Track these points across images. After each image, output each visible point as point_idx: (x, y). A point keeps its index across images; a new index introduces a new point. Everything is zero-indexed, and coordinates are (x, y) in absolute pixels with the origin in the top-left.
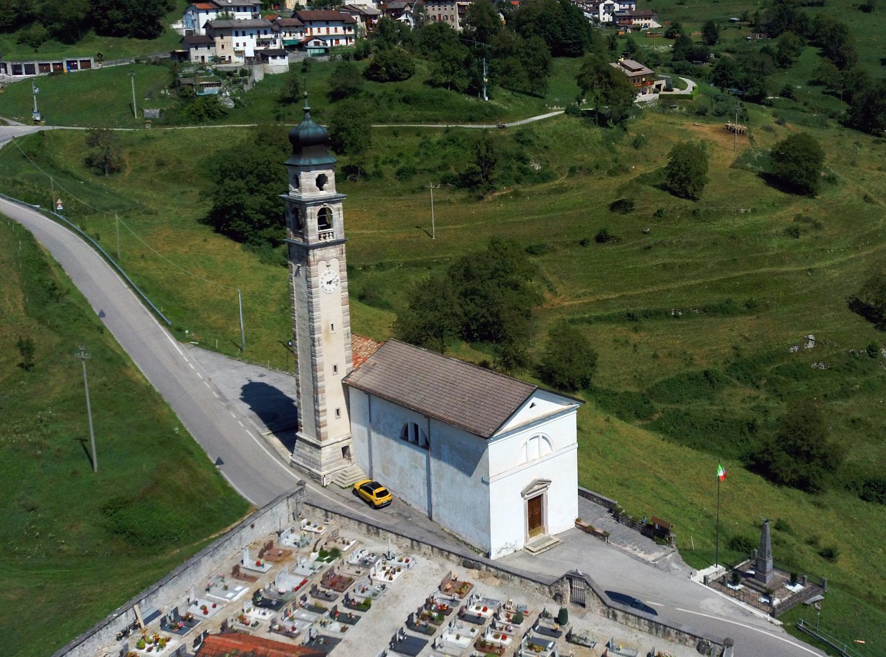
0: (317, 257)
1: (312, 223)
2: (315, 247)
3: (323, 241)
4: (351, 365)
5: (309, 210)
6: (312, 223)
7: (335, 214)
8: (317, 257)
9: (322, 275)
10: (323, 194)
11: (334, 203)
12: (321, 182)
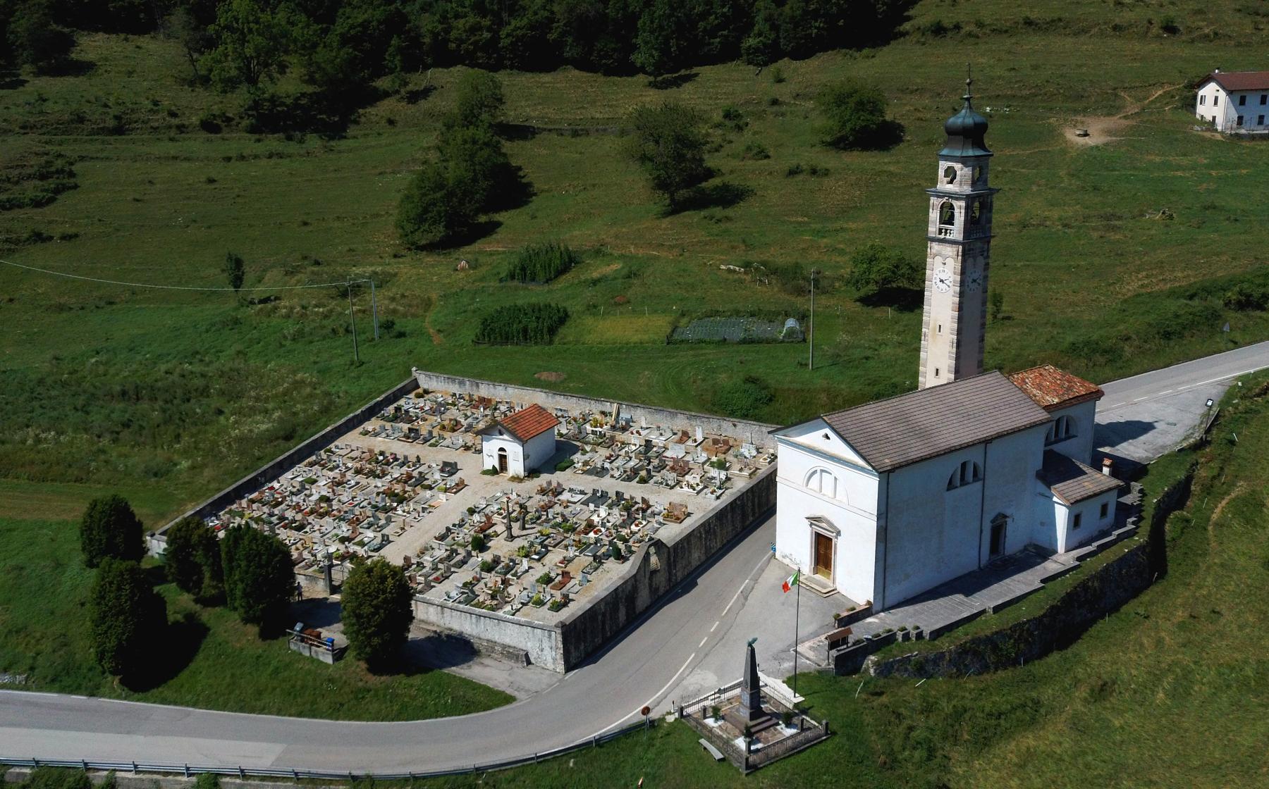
0: (934, 251)
1: (934, 215)
2: (933, 240)
3: (942, 236)
4: (952, 376)
5: (933, 200)
6: (934, 215)
7: (956, 212)
8: (934, 251)
9: (936, 271)
10: (950, 188)
11: (957, 199)
12: (951, 174)
